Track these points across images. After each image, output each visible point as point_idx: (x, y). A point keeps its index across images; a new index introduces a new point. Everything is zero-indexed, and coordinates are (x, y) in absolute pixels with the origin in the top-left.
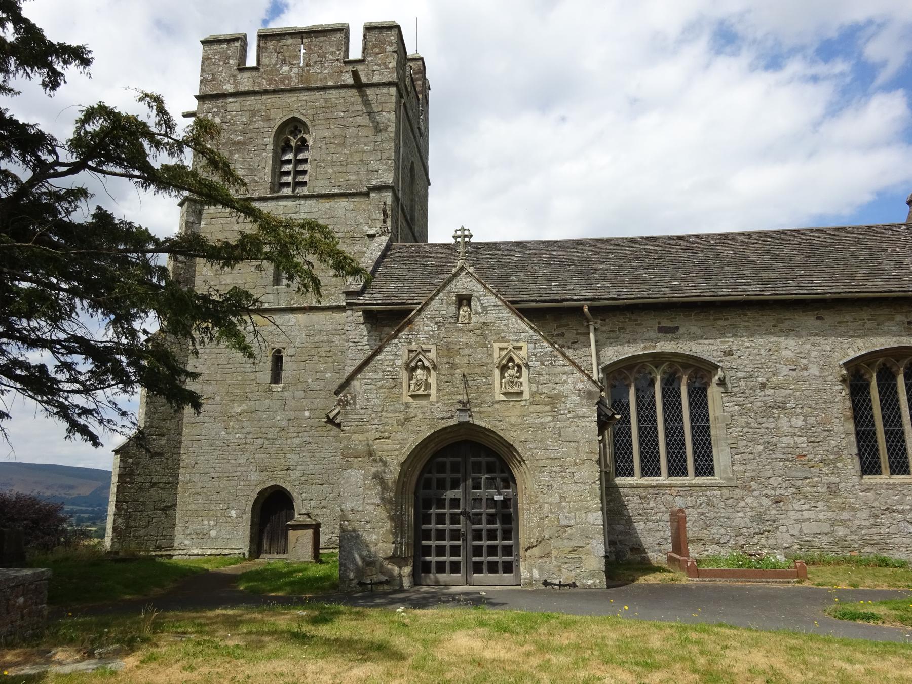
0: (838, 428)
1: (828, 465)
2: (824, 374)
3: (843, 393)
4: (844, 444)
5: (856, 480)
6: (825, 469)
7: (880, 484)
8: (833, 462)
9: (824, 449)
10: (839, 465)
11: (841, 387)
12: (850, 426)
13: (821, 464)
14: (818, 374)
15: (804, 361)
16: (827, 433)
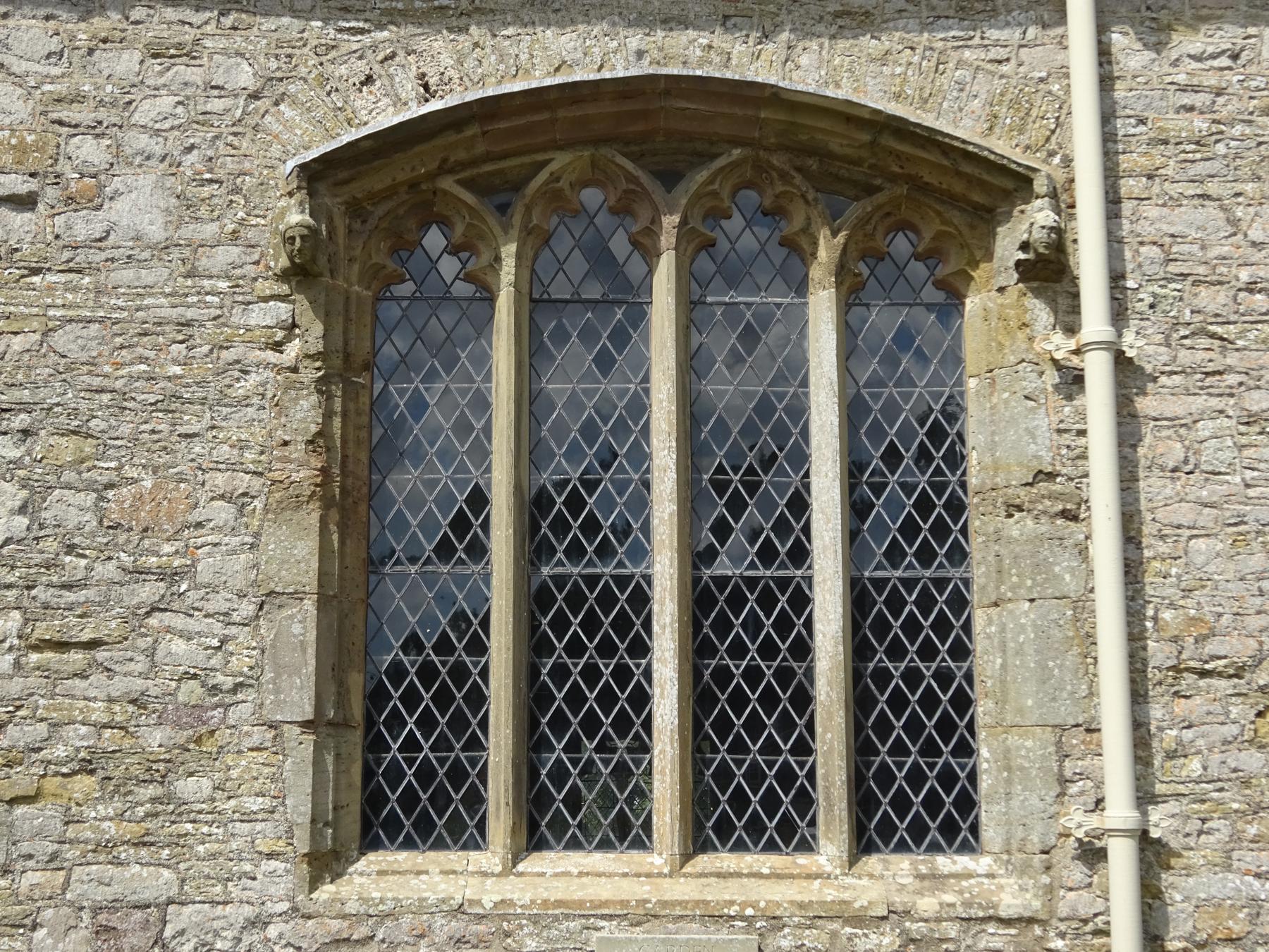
0: (223, 564)
1: (116, 788)
2: (188, 231)
3: (293, 350)
4: (241, 662)
5: (278, 882)
6: (103, 819)
7: (421, 907)
8: (159, 771)
9: (118, 686)
10: (191, 788)
11: (282, 310)
12: (296, 551)
13: (85, 783)
14: (156, 231)
15: (89, 150)
16: (149, 591)
